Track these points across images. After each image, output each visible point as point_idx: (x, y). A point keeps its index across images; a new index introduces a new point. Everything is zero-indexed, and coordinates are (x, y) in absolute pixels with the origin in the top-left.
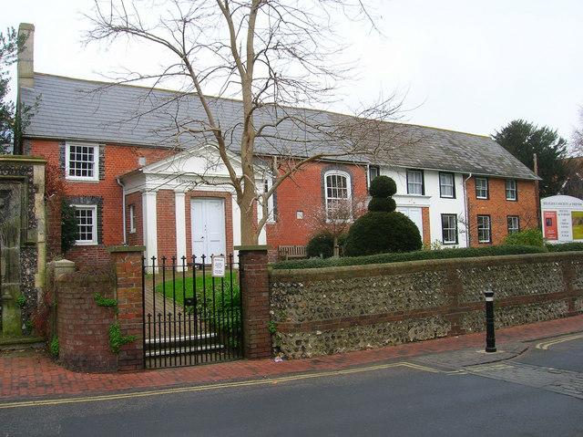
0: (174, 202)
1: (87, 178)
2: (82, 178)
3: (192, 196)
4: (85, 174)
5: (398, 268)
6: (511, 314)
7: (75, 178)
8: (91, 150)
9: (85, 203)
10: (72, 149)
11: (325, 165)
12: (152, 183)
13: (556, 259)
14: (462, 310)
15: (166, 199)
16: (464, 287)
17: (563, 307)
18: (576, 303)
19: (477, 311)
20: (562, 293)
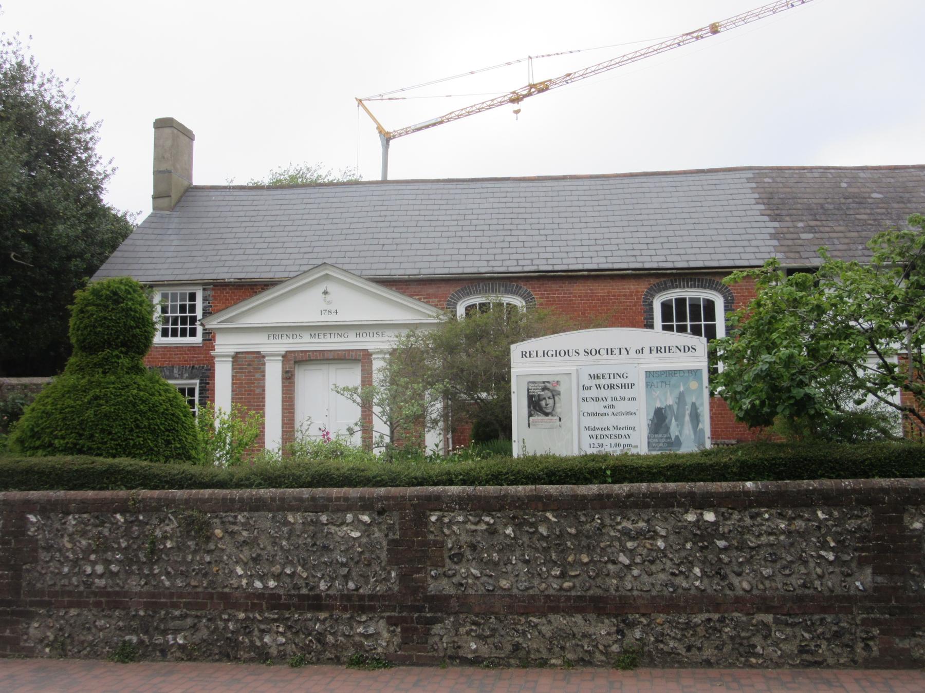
0: (264, 372)
1: (188, 340)
2: (179, 340)
3: (294, 362)
4: (183, 334)
5: (241, 500)
6: (176, 631)
7: (170, 340)
8: (193, 297)
9: (181, 377)
10: (165, 296)
11: (653, 281)
12: (225, 345)
13: (366, 505)
14: (32, 604)
15: (248, 367)
16: (44, 556)
17: (379, 633)
18: (437, 629)
19: (73, 612)
20: (372, 597)
